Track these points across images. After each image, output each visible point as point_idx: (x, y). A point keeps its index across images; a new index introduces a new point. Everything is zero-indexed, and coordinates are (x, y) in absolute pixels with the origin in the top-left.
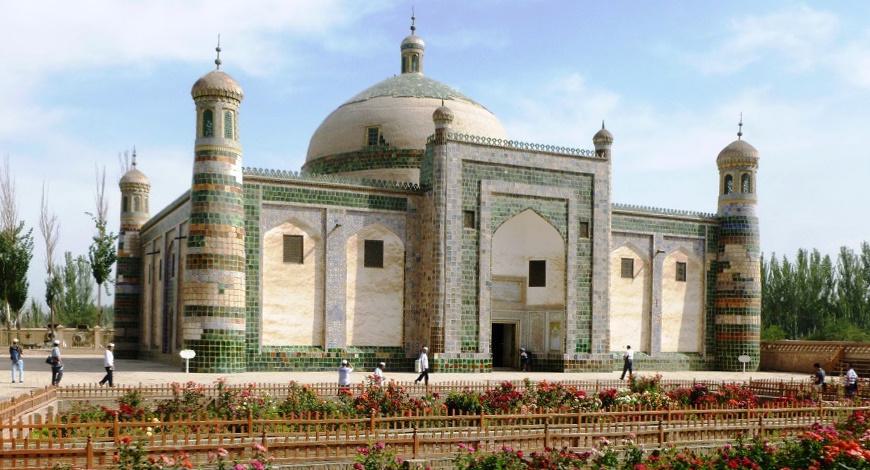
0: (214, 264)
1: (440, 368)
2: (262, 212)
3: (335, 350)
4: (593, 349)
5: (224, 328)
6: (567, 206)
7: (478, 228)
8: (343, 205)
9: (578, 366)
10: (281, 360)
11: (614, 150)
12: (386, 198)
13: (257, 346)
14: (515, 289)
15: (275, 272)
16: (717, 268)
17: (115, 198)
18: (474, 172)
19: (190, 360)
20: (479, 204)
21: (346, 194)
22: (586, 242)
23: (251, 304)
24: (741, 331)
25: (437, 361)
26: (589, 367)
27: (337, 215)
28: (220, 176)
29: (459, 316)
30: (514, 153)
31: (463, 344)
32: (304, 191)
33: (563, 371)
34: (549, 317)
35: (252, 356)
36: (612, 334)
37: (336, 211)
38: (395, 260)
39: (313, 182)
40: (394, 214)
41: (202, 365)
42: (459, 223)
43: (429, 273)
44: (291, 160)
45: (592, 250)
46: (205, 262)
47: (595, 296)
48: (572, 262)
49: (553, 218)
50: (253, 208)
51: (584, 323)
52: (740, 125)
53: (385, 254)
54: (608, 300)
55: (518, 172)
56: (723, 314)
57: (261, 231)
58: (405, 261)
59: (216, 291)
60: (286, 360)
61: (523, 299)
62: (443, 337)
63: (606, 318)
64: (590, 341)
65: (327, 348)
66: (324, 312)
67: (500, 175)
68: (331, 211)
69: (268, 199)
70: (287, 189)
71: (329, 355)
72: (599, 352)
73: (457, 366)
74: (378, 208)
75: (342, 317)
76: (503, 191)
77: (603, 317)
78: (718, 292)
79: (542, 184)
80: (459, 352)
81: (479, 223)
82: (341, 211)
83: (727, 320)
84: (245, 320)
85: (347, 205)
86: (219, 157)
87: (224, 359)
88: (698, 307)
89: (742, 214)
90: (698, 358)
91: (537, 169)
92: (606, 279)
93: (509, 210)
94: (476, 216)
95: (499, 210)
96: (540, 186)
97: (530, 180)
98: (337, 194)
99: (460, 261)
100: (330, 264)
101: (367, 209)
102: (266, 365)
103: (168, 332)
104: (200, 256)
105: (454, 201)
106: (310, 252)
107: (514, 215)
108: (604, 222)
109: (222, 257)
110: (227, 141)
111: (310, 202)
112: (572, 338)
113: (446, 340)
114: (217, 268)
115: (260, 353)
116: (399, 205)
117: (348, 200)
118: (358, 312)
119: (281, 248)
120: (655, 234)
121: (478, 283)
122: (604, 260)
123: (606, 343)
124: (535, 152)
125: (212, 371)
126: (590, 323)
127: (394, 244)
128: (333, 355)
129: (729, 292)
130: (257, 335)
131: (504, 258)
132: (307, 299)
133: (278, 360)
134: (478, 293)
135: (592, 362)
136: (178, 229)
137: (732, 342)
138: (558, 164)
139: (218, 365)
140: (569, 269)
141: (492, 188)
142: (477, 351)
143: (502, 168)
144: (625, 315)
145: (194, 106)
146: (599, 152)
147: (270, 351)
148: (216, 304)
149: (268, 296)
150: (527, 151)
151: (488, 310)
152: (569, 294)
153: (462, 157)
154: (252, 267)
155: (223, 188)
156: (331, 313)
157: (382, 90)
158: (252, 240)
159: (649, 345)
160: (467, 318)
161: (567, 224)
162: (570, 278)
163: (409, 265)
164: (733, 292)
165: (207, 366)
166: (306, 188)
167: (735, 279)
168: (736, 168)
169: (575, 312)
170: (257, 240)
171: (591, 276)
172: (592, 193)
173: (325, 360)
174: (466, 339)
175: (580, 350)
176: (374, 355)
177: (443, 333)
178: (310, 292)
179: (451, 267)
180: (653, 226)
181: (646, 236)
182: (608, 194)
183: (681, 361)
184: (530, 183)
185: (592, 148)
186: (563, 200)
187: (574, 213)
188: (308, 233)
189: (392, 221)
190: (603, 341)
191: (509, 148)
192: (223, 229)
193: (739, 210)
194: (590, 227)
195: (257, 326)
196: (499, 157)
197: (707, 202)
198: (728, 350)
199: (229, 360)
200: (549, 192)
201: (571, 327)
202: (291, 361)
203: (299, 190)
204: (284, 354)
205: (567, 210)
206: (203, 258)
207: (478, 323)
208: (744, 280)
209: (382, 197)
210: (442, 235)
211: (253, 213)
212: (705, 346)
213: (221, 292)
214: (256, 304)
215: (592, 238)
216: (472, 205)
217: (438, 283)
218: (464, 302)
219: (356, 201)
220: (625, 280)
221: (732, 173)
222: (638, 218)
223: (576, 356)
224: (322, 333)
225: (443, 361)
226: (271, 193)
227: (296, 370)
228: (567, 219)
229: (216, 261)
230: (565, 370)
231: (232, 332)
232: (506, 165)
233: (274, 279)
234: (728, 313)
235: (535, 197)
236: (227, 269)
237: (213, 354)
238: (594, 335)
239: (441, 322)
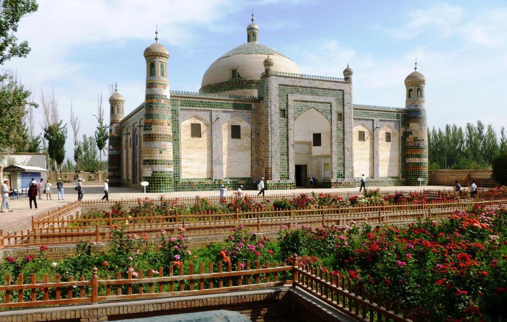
0: (157, 139)
1: (270, 188)
2: (180, 113)
4: (346, 176)
5: (163, 170)
6: (331, 106)
7: (287, 118)
8: (220, 108)
9: (338, 185)
10: (191, 185)
11: (353, 78)
12: (242, 104)
13: (179, 179)
14: (306, 148)
15: (187, 142)
16: (406, 135)
17: (107, 107)
18: (284, 90)
19: (146, 186)
20: (287, 106)
21: (221, 103)
22: (340, 123)
23: (176, 158)
24: (419, 166)
25: (268, 184)
26: (344, 185)
27: (217, 113)
28: (159, 95)
29: (278, 161)
30: (304, 80)
31: (281, 175)
32: (201, 102)
34: (323, 161)
35: (177, 184)
36: (355, 169)
37: (217, 111)
38: (247, 135)
39: (205, 97)
40: (245, 112)
41: (152, 189)
42: (278, 116)
43: (263, 141)
44: (194, 87)
45: (344, 128)
46: (152, 138)
47: (346, 150)
48: (334, 134)
49: (324, 112)
50: (176, 111)
51: (341, 163)
52: (416, 64)
53: (242, 132)
54: (352, 152)
56: (410, 157)
58: (252, 135)
59: (158, 152)
61: (310, 152)
62: (271, 172)
63: (351, 161)
64: (344, 173)
66: (212, 161)
67: (297, 91)
68: (214, 111)
69: (183, 106)
70: (192, 101)
71: (215, 183)
73: (278, 186)
74: (238, 109)
75: (221, 164)
77: (350, 160)
78: (406, 147)
79: (318, 95)
80: (279, 179)
81: (287, 115)
82: (219, 111)
83: (412, 160)
84: (173, 166)
85: (222, 108)
86: (158, 86)
87: (163, 186)
88: (397, 154)
89: (418, 108)
90: (398, 180)
91: (315, 88)
92: (351, 142)
93: (302, 109)
94: (286, 112)
95: (297, 109)
96: (317, 96)
97: (312, 93)
98: (217, 103)
99: (278, 134)
100: (214, 138)
101: (232, 110)
102: (184, 188)
103: (135, 173)
104: (150, 135)
106: (204, 132)
107: (305, 111)
108: (349, 114)
109: (161, 135)
110: (162, 78)
111: (203, 107)
112: (335, 171)
114: (158, 141)
116: (248, 107)
118: (229, 161)
119: (190, 130)
120: (374, 119)
121: (288, 145)
122: (350, 132)
123: (352, 173)
124: (314, 80)
125: (157, 192)
126: (344, 164)
127: (246, 127)
129: (412, 147)
130: (179, 174)
131: (301, 132)
132: (203, 155)
133: (190, 186)
134: (288, 150)
135: (345, 183)
136: (138, 122)
138: (326, 85)
139: (160, 189)
140: (333, 137)
141: (293, 98)
142: (288, 179)
144: (361, 159)
145: (146, 61)
146: (346, 79)
147: (186, 181)
148: (158, 158)
149: (184, 154)
150: (311, 79)
151: (293, 158)
152: (333, 149)
154: (176, 140)
155: (160, 101)
156: (215, 161)
157: (238, 51)
159: (373, 174)
160: (283, 162)
161: (331, 115)
162: (333, 142)
163: (253, 137)
164: (414, 146)
165: (155, 189)
166: (201, 100)
167: (414, 140)
168: (414, 85)
170: (178, 127)
171: (344, 140)
172: (343, 99)
173: (213, 185)
176: (237, 182)
177: (271, 170)
178: (205, 151)
179: (274, 138)
181: (370, 120)
182: (351, 100)
183: (389, 181)
184: (312, 95)
185: (343, 77)
186: (329, 103)
187: (334, 110)
188: (203, 123)
189: (245, 115)
190: (351, 173)
191: (301, 78)
192: (161, 122)
193: (416, 106)
194: (343, 116)
195: (179, 169)
196: (297, 83)
197: (400, 102)
198: (412, 175)
199: (165, 186)
200: (322, 99)
201: (335, 166)
202: (196, 186)
204: (193, 183)
205: (331, 108)
206: (152, 136)
207: (288, 165)
208: (419, 140)
209: (239, 104)
210: (269, 122)
211: (175, 113)
212: (401, 174)
213: (161, 152)
214: (178, 158)
215: (344, 122)
216: (284, 106)
217: (268, 146)
218: (281, 155)
220: (360, 142)
221: (412, 88)
222: (366, 111)
223: (337, 180)
224: (211, 171)
227: (198, 191)
228: (331, 113)
229: (158, 137)
230: (332, 187)
231: (167, 172)
232: (300, 87)
233: (187, 145)
234: (412, 157)
235: (315, 102)
236: (164, 141)
237: (157, 183)
238: (346, 169)
239: (270, 165)
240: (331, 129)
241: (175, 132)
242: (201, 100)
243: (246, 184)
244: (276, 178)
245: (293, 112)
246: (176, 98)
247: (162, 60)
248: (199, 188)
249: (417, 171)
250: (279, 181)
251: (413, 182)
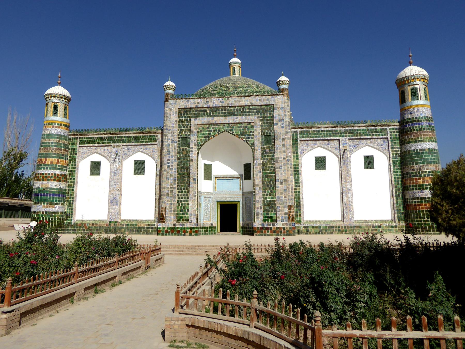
2: (80, 151)
6: (253, 127)
7: (189, 147)
8: (120, 143)
13: (71, 220)
19: (34, 227)
21: (122, 137)
26: (274, 232)
27: (117, 148)
31: (179, 217)
33: (253, 235)
37: (117, 146)
42: (176, 145)
49: (243, 135)
50: (74, 149)
55: (216, 111)
67: (204, 114)
68: (114, 147)
70: (91, 138)
71: (110, 224)
72: (282, 221)
74: (140, 142)
76: (205, 123)
79: (234, 115)
80: (175, 222)
82: (119, 146)
85: (123, 142)
91: (230, 107)
93: (210, 134)
98: (118, 137)
99: (175, 166)
105: (173, 132)
107: (214, 137)
111: (103, 143)
113: (166, 215)
115: (73, 224)
117: (123, 140)
128: (112, 225)
130: (72, 214)
135: (277, 228)
137: (416, 212)
143: (206, 109)
153: (178, 107)
158: (72, 165)
160: (181, 201)
169: (261, 194)
174: (180, 214)
175: (268, 221)
180: (338, 133)
184: (225, 116)
195: (72, 209)
200: (239, 119)
203: (98, 137)
204: (85, 224)
209: (143, 136)
214: (73, 198)
218: (179, 192)
219: (128, 140)
223: (263, 225)
225: (164, 228)
226: (83, 141)
230: (255, 234)
235: (229, 123)
240: (253, 155)
241: (71, 171)
242: (101, 136)
243: (147, 228)
244: (170, 220)
245: (197, 139)
246: (77, 137)
247: (55, 101)
249: (419, 211)
250: (174, 225)
251: (416, 227)
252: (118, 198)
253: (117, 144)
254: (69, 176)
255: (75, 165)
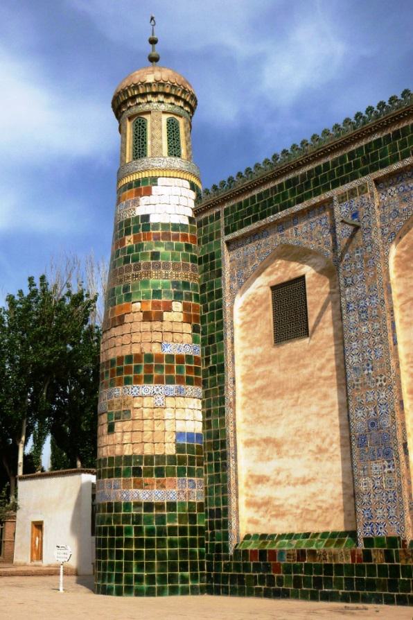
3: (380, 540)
8: (364, 173)
21: (368, 146)
32: (289, 183)
37: (352, 193)
57: (226, 294)
60: (277, 570)
65: (361, 534)
68: (342, 198)
69: (234, 230)
70: (260, 196)
71: (367, 556)
82: (363, 189)
85: (374, 169)
98: (351, 155)
111: (300, 201)
115: (231, 552)
117: (374, 157)
119: (270, 315)
128: (378, 558)
132: (319, 417)
149: (243, 424)
154: (208, 372)
156: (362, 444)
173: (360, 568)
178: (325, 396)
188: (314, 266)
199: (119, 565)
202: (288, 569)
204: (273, 553)
213: (111, 429)
214: (224, 444)
231: (127, 506)
233: (259, 383)
241: (211, 340)
247: (135, 110)
248: (297, 582)
252: (387, 422)
253: (354, 184)
254: (207, 360)
255: (220, 315)
